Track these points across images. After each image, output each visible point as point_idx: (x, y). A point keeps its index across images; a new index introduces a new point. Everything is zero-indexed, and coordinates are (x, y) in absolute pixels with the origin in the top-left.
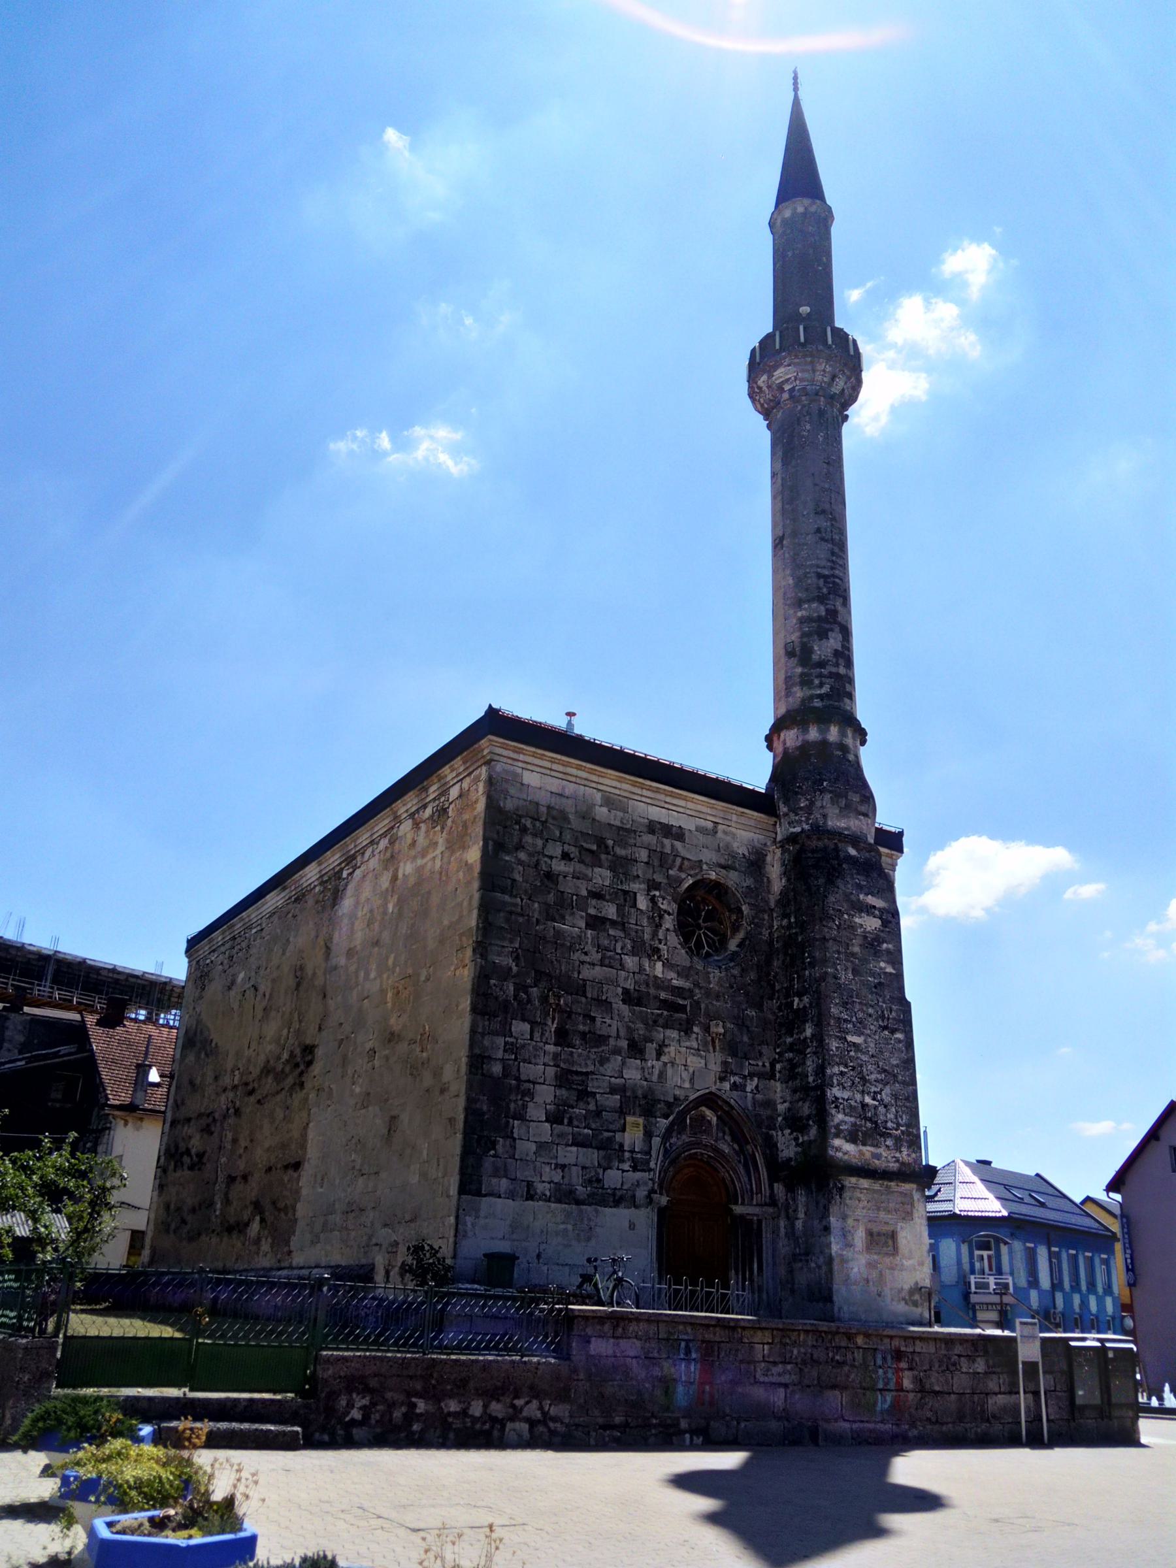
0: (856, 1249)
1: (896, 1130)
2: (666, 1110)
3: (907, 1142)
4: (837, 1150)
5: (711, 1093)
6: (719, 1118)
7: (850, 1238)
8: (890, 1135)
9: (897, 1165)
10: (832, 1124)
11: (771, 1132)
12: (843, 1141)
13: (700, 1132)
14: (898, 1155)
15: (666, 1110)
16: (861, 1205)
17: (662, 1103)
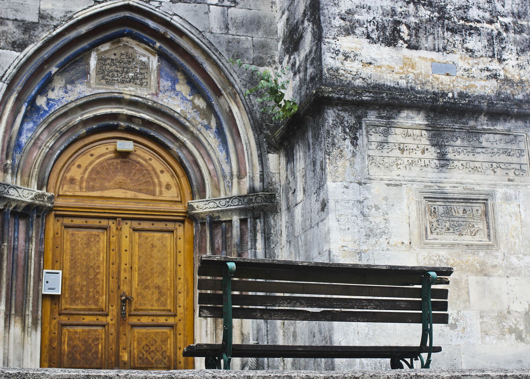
0: (394, 240)
1: (491, 22)
2: (18, 35)
3: (515, 42)
4: (346, 57)
5: (127, 7)
6: (162, 56)
7: (377, 219)
8: (474, 31)
9: (493, 83)
10: (334, 10)
11: (261, 70)
12: (365, 41)
13: (123, 82)
14: (495, 65)
15: (18, 35)
16: (406, 157)
17: (10, 23)
